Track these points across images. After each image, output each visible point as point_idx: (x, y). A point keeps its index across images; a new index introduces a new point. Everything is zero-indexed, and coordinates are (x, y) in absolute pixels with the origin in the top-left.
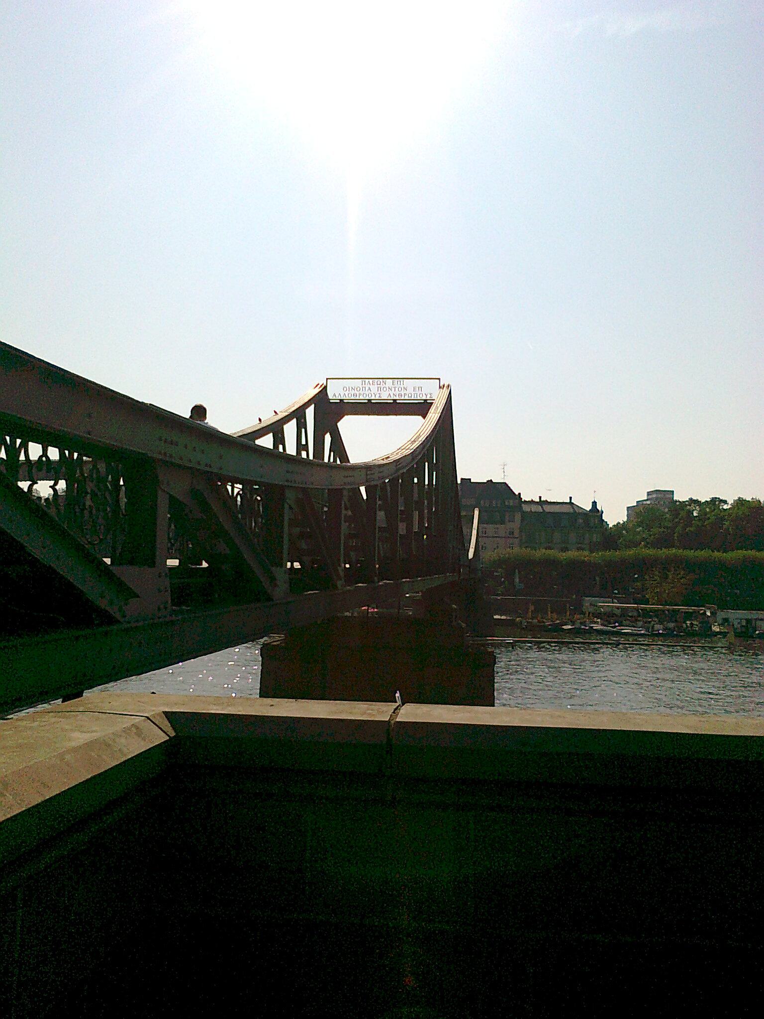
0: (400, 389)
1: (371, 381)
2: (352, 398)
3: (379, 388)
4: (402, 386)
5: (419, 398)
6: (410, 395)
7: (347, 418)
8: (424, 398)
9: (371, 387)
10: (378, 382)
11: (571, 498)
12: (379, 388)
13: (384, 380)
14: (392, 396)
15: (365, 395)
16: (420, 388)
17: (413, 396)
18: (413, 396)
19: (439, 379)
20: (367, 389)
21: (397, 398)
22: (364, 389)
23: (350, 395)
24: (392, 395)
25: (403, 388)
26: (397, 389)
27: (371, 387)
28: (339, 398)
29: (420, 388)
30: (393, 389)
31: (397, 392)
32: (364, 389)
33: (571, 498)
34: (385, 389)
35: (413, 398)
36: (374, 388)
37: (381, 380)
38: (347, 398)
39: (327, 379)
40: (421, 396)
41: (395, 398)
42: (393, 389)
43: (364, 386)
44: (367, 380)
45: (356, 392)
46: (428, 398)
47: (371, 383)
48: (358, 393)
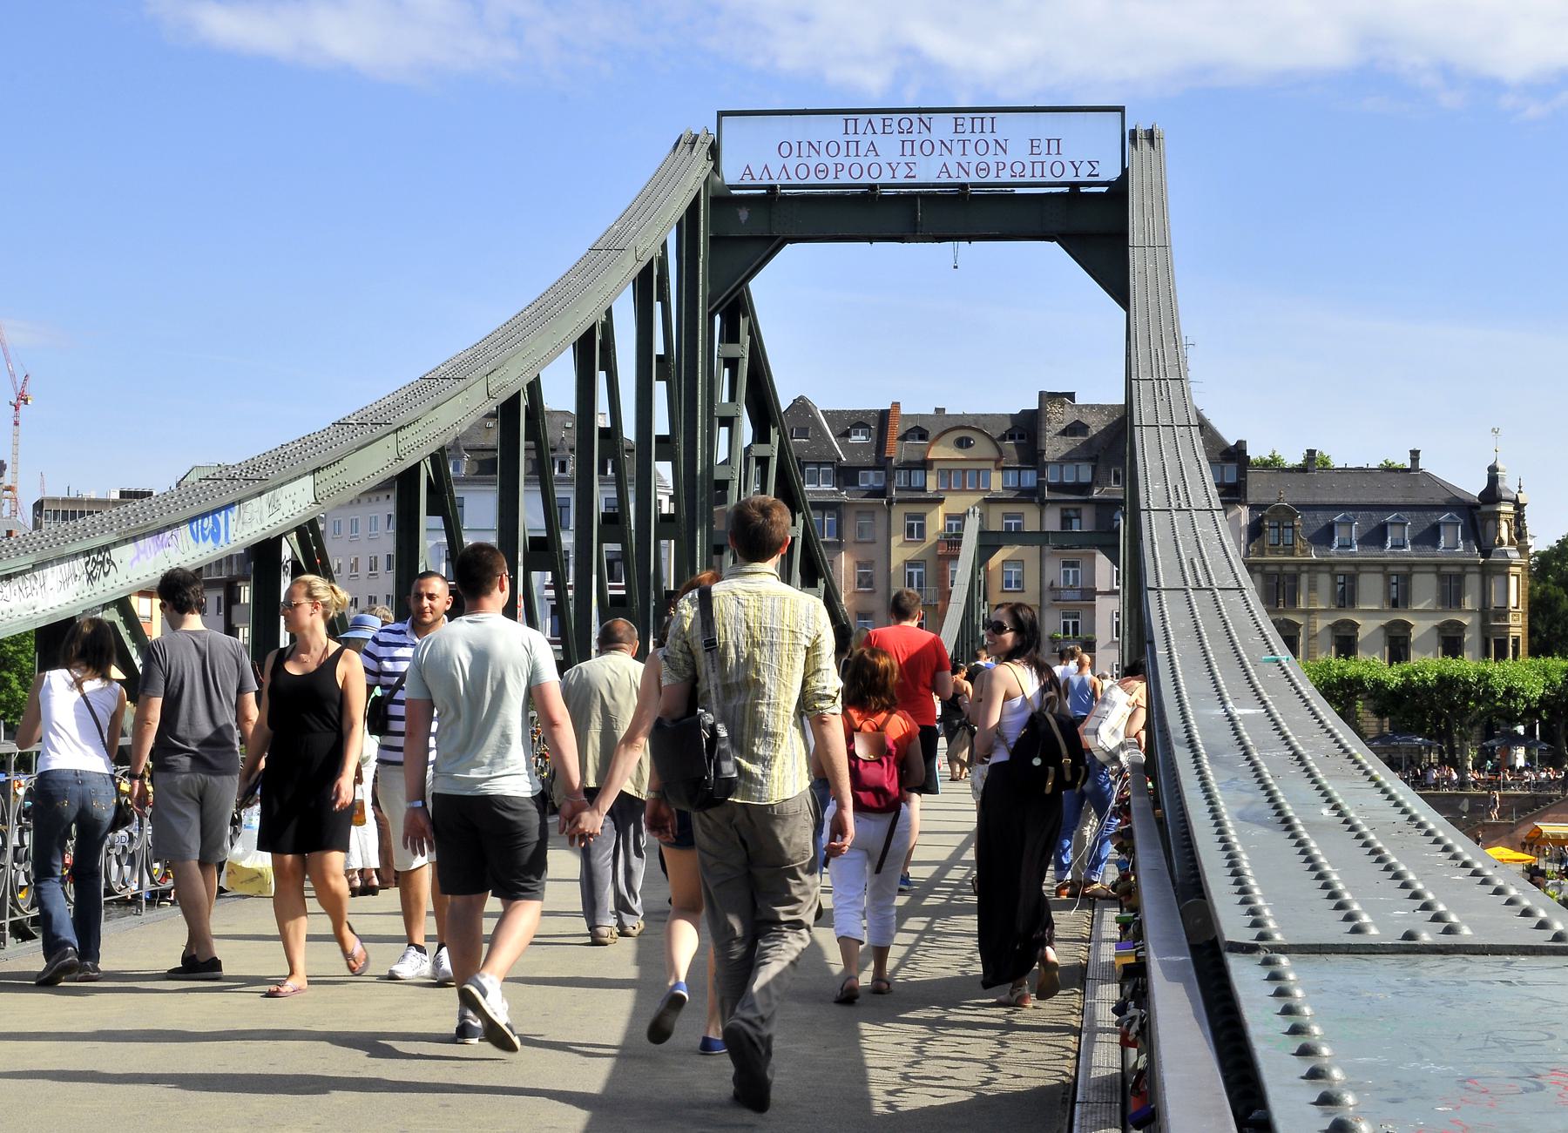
0: (982, 147)
1: (876, 119)
2: (812, 180)
3: (908, 145)
4: (990, 138)
5: (1049, 178)
6: (1018, 168)
7: (792, 256)
8: (1069, 176)
9: (879, 140)
10: (905, 125)
11: (1415, 455)
12: (908, 145)
13: (924, 116)
14: (953, 173)
15: (856, 171)
16: (1054, 144)
17: (1028, 172)
18: (1028, 172)
19: (1121, 109)
20: (862, 151)
21: (974, 179)
22: (852, 146)
23: (802, 172)
24: (954, 171)
25: (992, 144)
26: (970, 147)
27: (879, 140)
28: (766, 181)
29: (1054, 144)
30: (957, 148)
31: (974, 159)
32: (852, 146)
33: (1415, 455)
34: (927, 148)
35: (1027, 179)
36: (889, 147)
37: (914, 117)
38: (795, 181)
39: (721, 114)
40: (1058, 169)
41: (964, 179)
42: (957, 148)
43: (851, 137)
44: (863, 119)
45: (824, 158)
46: (1083, 178)
47: (879, 129)
48: (830, 163)
